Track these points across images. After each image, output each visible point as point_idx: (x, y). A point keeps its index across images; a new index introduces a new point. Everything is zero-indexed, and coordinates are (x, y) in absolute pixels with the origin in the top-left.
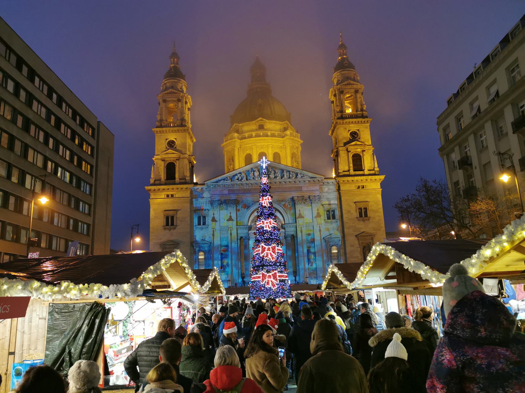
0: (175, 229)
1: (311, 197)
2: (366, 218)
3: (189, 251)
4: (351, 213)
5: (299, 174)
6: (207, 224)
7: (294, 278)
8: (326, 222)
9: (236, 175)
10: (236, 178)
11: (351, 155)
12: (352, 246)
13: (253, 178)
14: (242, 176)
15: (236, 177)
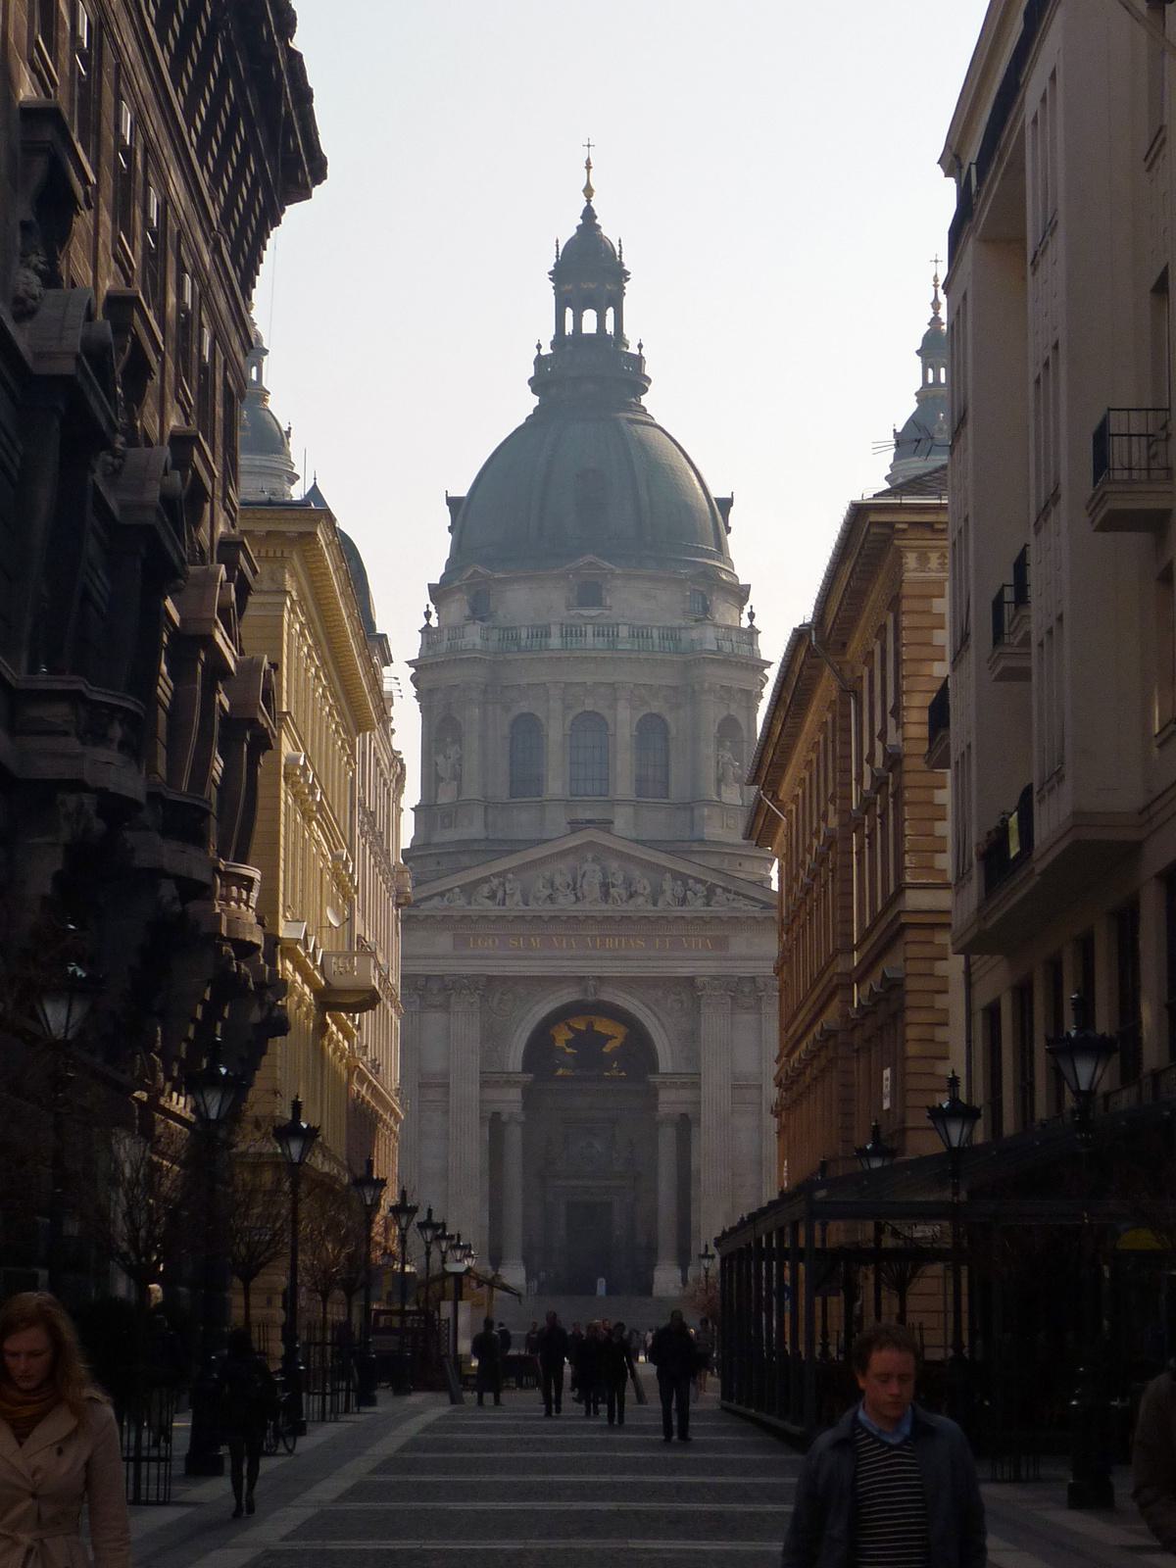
1: (757, 979)
5: (719, 891)
7: (679, 1273)
13: (550, 897)
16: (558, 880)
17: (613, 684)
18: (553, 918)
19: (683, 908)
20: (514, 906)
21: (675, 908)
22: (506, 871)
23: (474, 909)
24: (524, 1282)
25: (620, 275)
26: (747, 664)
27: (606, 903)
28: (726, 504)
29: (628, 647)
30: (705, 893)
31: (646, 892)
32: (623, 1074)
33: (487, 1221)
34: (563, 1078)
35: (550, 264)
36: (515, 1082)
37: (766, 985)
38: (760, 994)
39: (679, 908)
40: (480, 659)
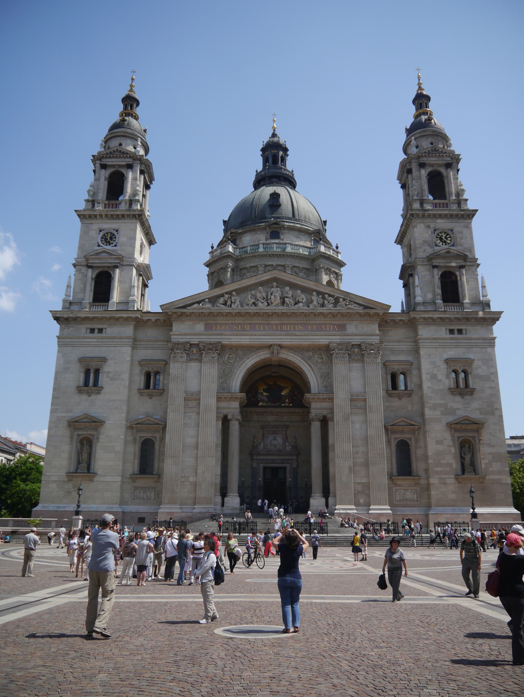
0: (98, 393)
1: (362, 345)
2: (467, 390)
3: (123, 437)
4: (439, 377)
5: (341, 300)
6: (161, 387)
7: (324, 500)
8: (390, 395)
9: (222, 295)
10: (221, 302)
11: (437, 273)
12: (439, 442)
13: (254, 303)
14: (233, 298)
15: (222, 300)
16: (258, 295)
17: (284, 265)
18: (256, 314)
19: (323, 308)
20: (236, 307)
21: (318, 308)
22: (232, 291)
23: (215, 309)
24: (238, 506)
25: (285, 150)
26: (337, 262)
27: (283, 306)
28: (325, 222)
29: (290, 251)
30: (334, 301)
31: (304, 301)
32: (291, 405)
33: (219, 472)
34: (262, 406)
35: (261, 146)
36: (236, 398)
37: (366, 348)
38: (363, 352)
39: (321, 308)
40: (231, 256)
